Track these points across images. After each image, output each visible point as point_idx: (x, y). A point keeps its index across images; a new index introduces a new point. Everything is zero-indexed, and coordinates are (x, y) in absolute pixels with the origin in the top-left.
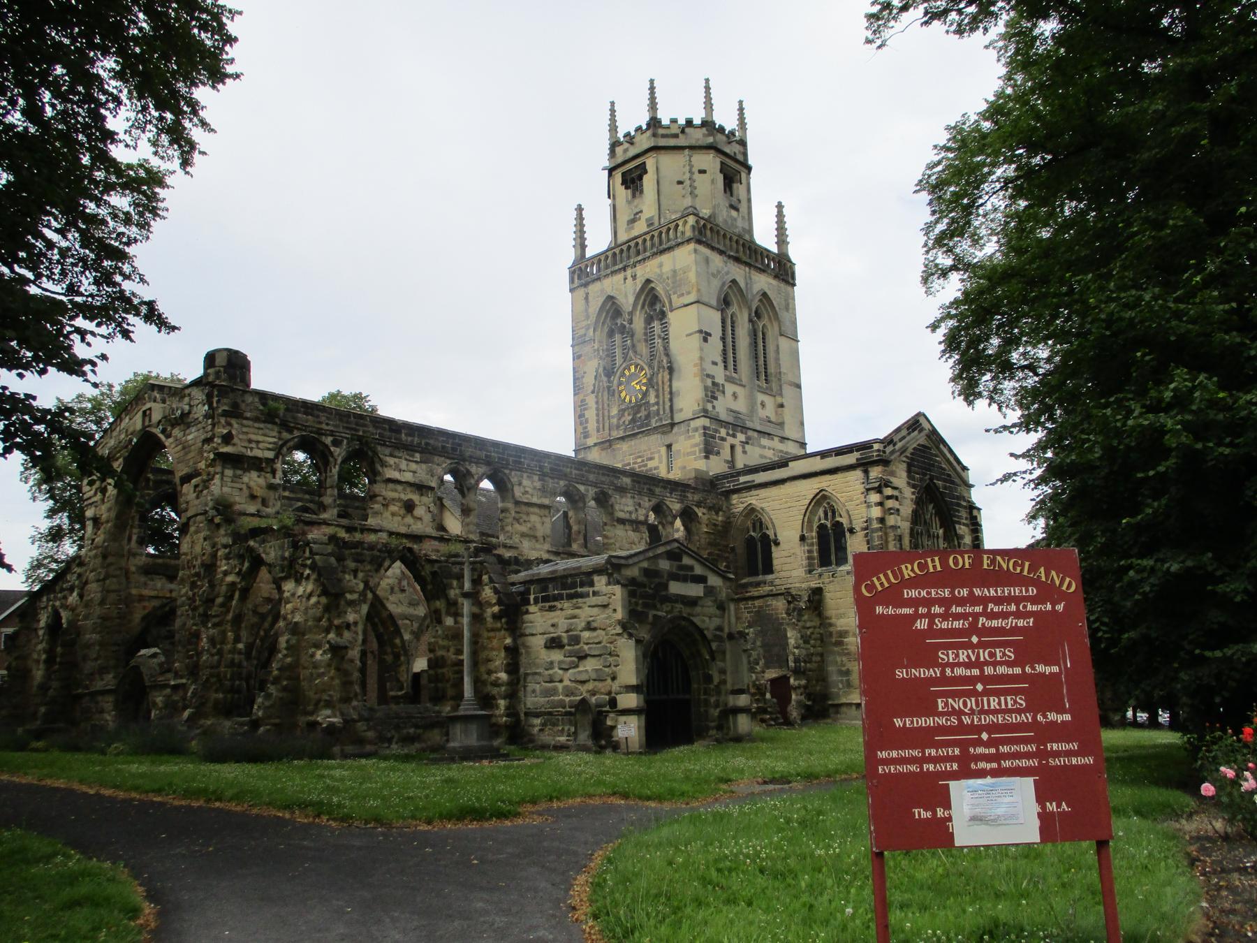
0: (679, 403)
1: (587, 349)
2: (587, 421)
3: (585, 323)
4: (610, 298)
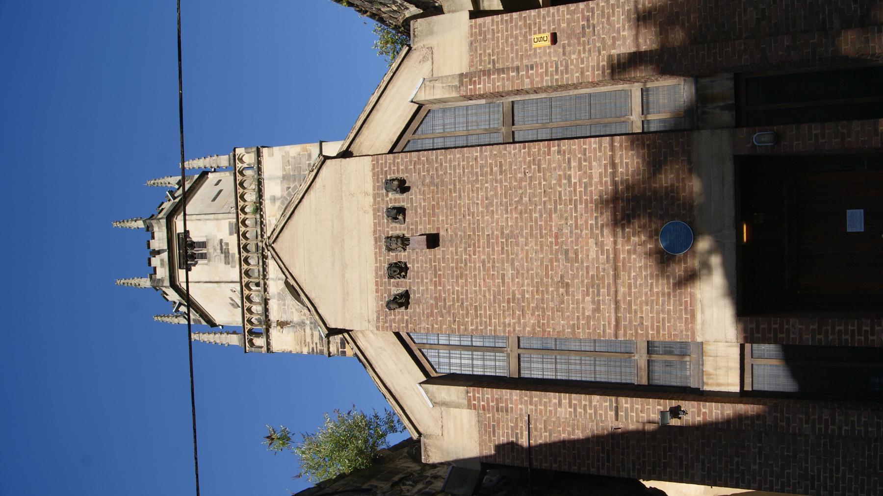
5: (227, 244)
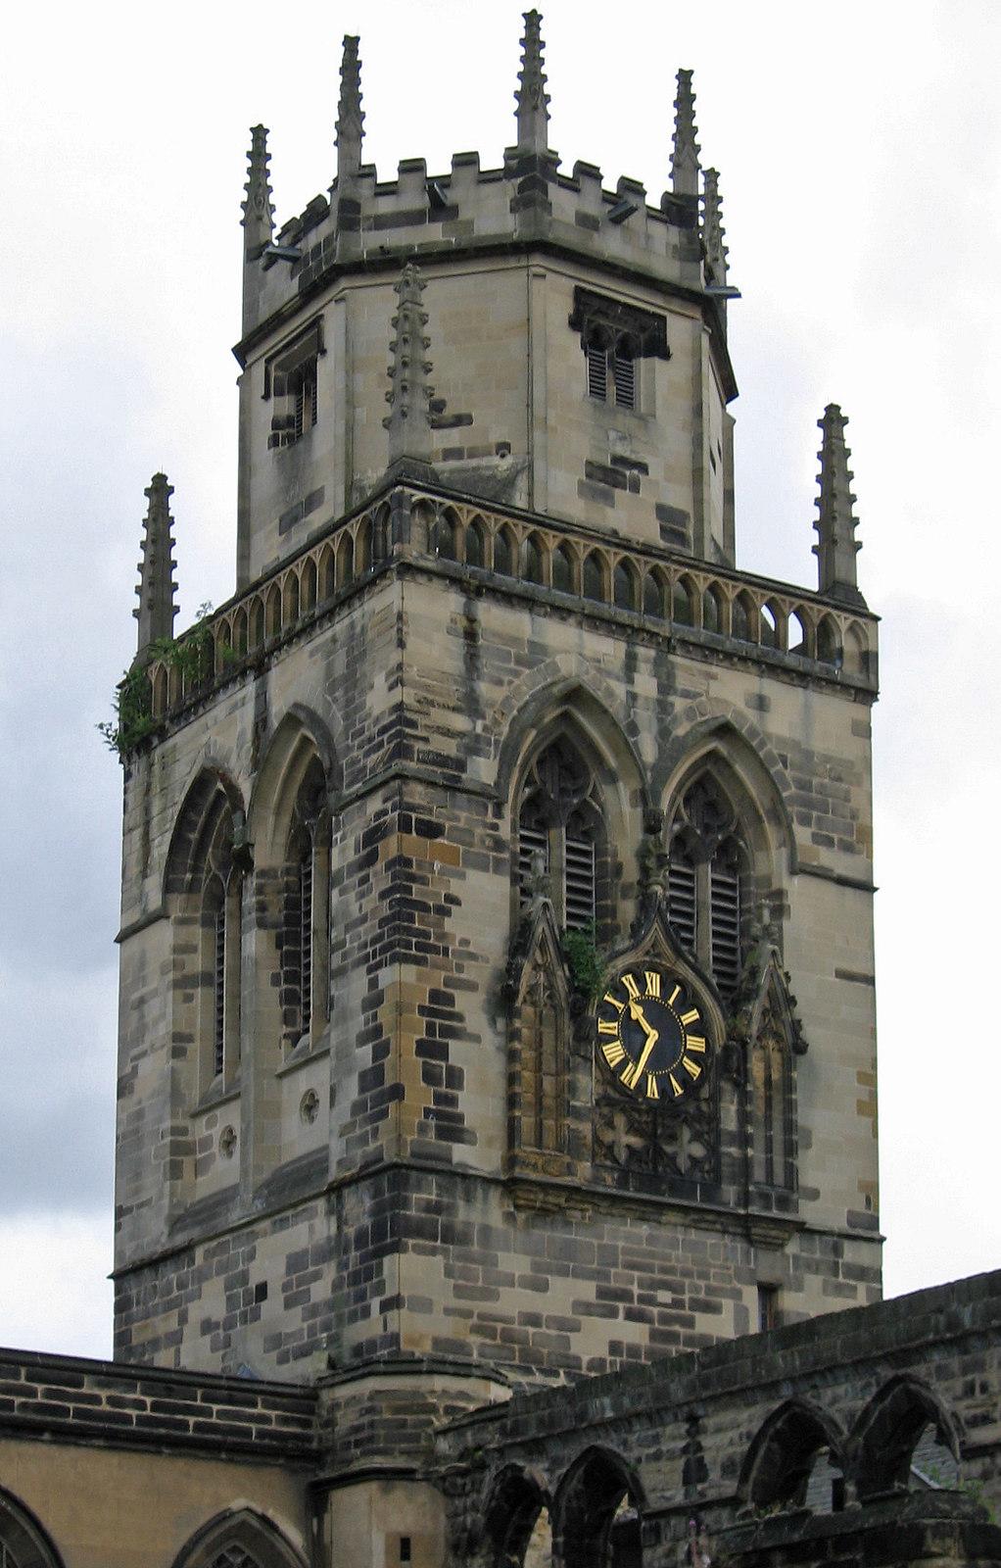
0: (812, 1171)
1: (461, 816)
2: (455, 1078)
3: (460, 723)
4: (576, 695)
5: (635, 487)
